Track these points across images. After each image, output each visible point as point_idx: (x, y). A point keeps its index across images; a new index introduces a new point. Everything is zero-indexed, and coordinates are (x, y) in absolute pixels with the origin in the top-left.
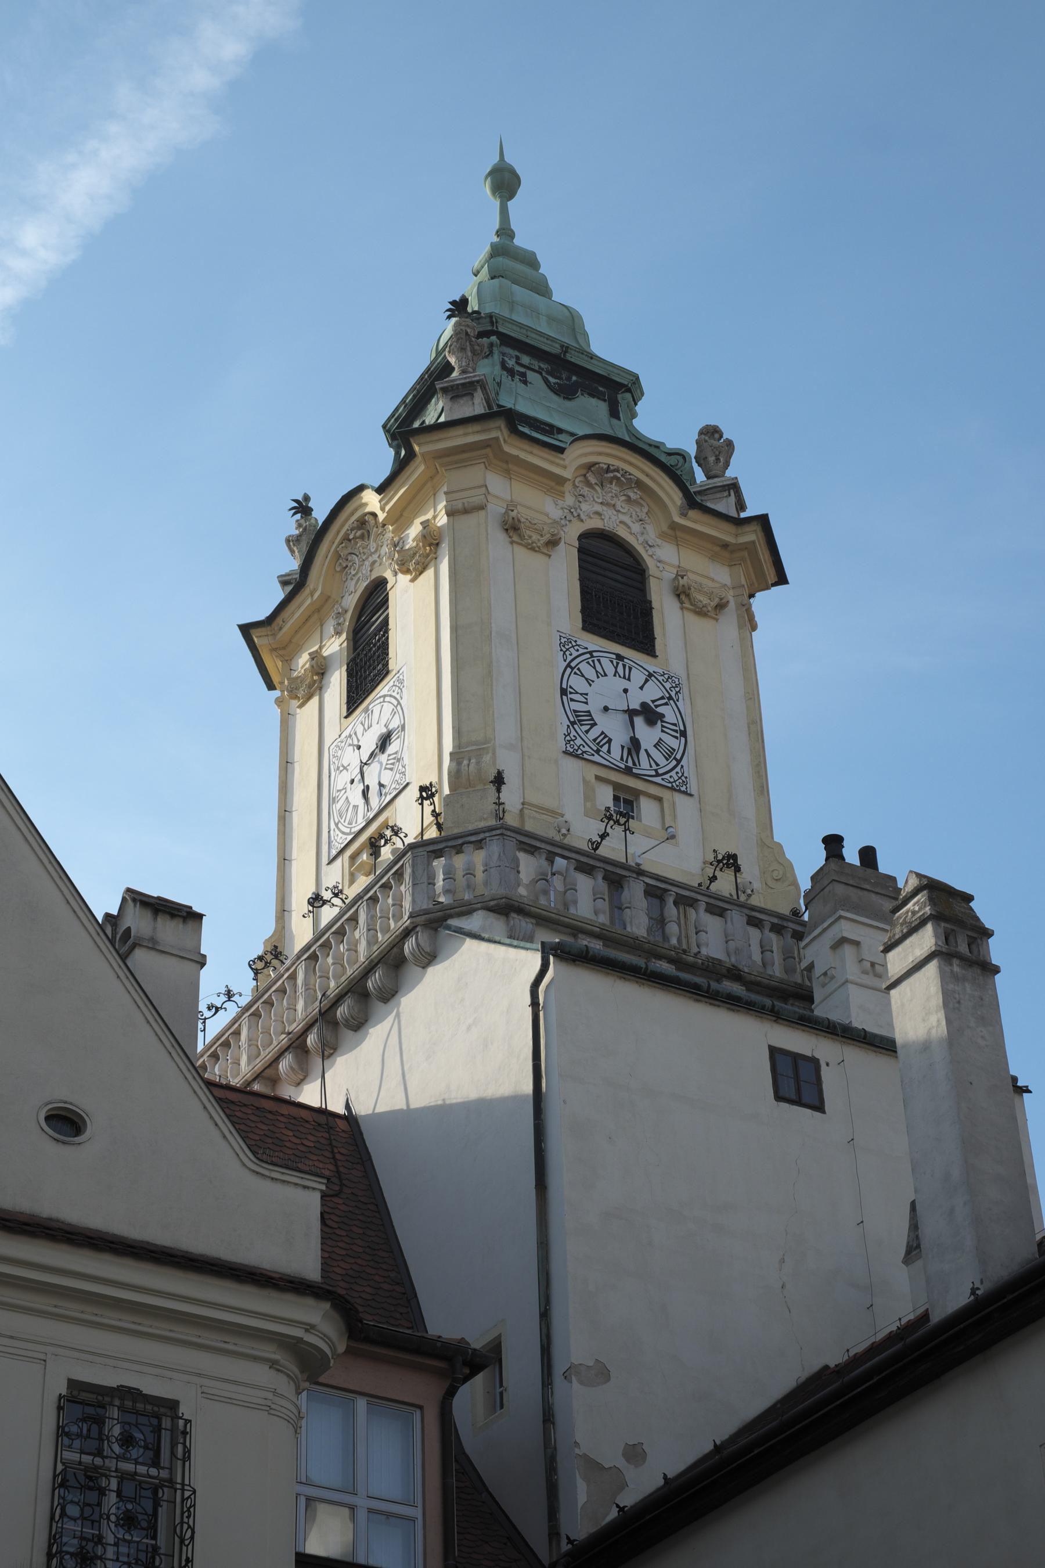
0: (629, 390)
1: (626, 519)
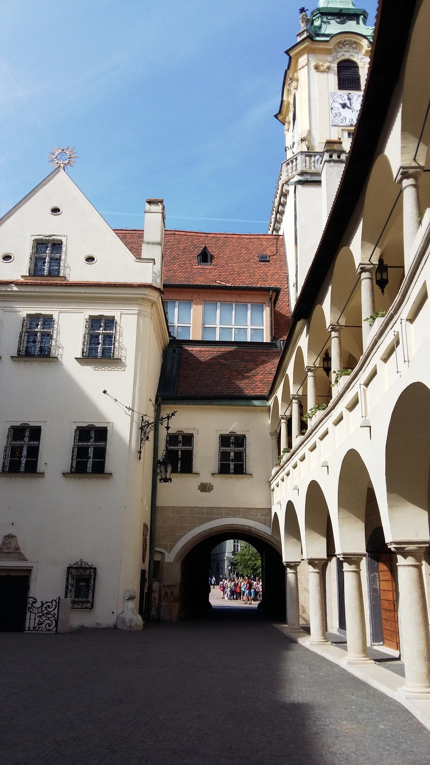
0: (361, 15)
1: (352, 54)
